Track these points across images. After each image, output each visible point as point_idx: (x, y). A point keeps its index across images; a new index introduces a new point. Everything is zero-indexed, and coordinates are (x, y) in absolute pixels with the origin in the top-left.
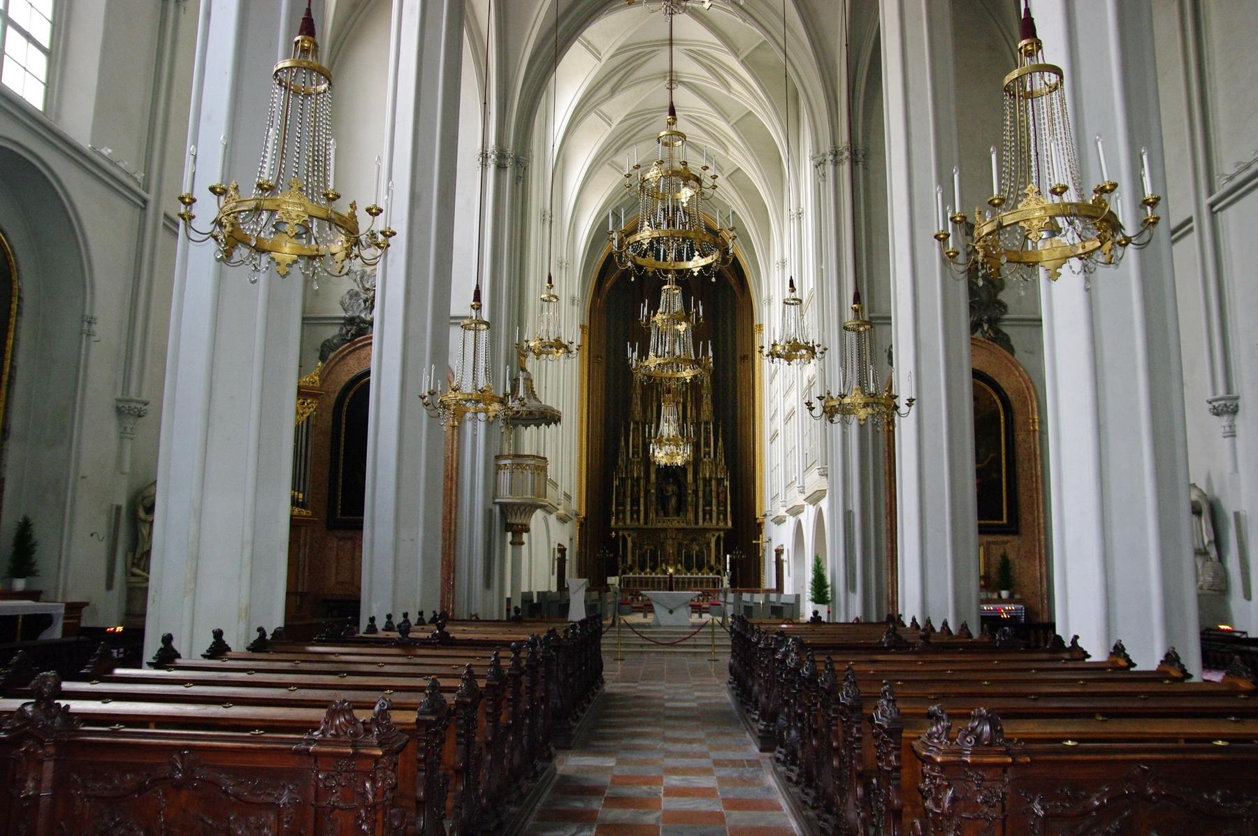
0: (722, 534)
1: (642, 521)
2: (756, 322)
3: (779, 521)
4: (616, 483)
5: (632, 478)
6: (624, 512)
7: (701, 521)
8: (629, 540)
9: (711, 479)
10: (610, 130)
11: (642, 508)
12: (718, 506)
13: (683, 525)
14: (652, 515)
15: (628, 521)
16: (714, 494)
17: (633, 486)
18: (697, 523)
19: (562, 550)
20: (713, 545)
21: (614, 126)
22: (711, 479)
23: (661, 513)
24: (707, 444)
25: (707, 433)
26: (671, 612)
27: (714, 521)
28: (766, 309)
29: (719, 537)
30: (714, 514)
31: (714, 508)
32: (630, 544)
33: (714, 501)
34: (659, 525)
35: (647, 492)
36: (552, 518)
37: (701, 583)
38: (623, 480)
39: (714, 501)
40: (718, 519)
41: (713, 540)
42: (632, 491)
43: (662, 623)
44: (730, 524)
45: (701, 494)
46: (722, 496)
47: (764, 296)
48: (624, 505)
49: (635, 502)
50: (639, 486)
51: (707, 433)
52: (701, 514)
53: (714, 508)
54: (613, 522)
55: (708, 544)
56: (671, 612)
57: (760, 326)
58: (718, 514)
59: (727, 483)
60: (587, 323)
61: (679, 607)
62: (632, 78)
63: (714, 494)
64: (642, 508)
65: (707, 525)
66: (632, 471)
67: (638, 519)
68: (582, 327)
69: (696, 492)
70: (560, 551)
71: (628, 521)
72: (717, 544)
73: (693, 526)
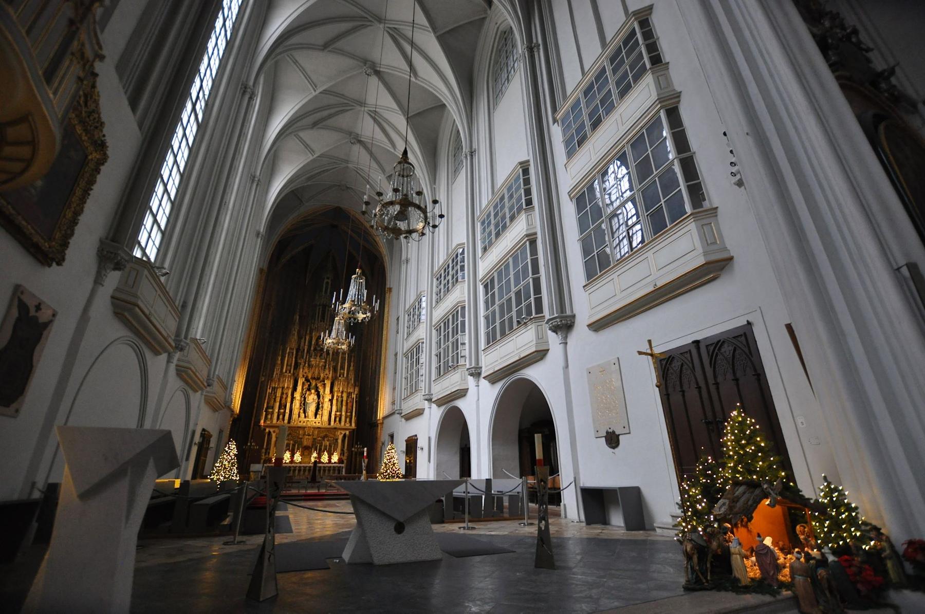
0: (347, 433)
1: (286, 421)
2: (388, 286)
3: (418, 413)
4: (269, 391)
5: (283, 388)
6: (272, 413)
7: (332, 423)
8: (274, 435)
9: (342, 392)
10: (314, 94)
11: (288, 411)
12: (347, 412)
13: (318, 425)
14: (295, 416)
15: (275, 421)
16: (344, 403)
17: (282, 393)
18: (330, 424)
19: (206, 436)
20: (340, 441)
21: (318, 92)
22: (342, 392)
23: (302, 415)
24: (342, 368)
25: (343, 359)
26: (400, 528)
27: (343, 423)
28: (404, 267)
29: (345, 435)
30: (343, 418)
31: (343, 413)
32: (274, 439)
33: (344, 408)
34: (300, 424)
35: (293, 398)
36: (197, 398)
37: (329, 470)
38: (274, 389)
39: (344, 408)
40: (346, 421)
41: (341, 437)
42: (281, 398)
43: (376, 561)
44: (353, 425)
45: (334, 402)
46: (349, 405)
47: (404, 258)
48: (273, 408)
49: (282, 406)
50: (287, 394)
51: (343, 359)
52: (333, 417)
53: (343, 413)
54: (262, 421)
55: (337, 440)
56: (400, 528)
57: (390, 289)
58: (346, 418)
59: (354, 396)
60: (265, 268)
61: (413, 519)
62: (324, 123)
63: (344, 403)
64: (288, 411)
65: (338, 426)
66: (284, 382)
67: (283, 419)
68: (261, 271)
69: (331, 401)
70: (202, 435)
71: (275, 421)
72: (343, 441)
73: (326, 425)
